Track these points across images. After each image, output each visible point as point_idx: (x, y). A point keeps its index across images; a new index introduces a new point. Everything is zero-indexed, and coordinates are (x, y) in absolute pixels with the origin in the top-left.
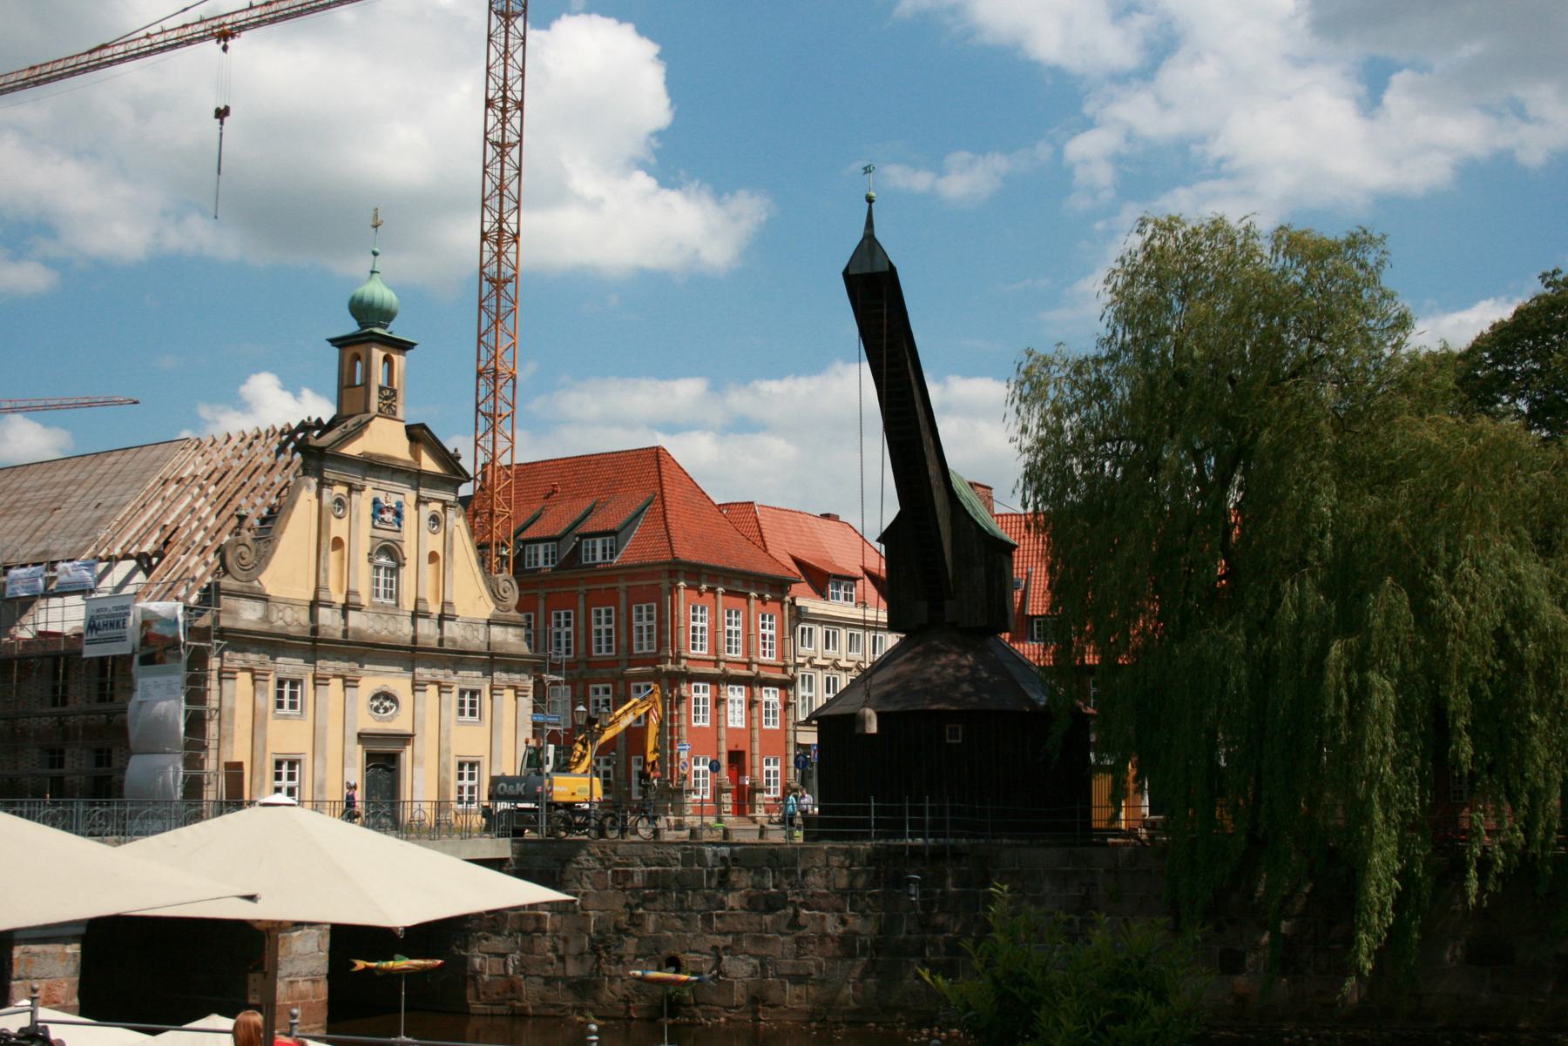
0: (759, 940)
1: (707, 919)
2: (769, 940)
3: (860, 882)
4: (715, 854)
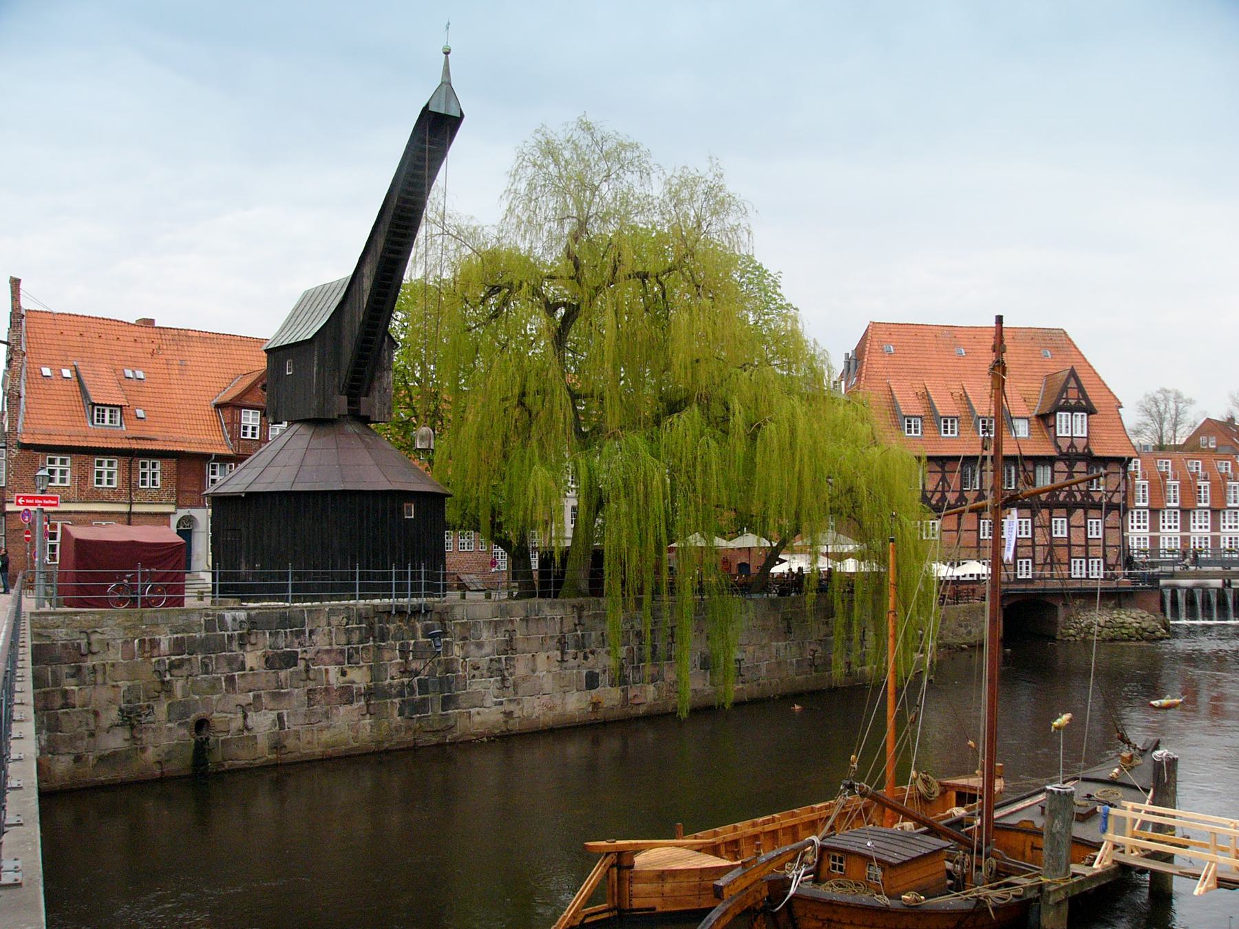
0: (276, 696)
1: (230, 680)
2: (285, 694)
3: (356, 637)
4: (234, 619)
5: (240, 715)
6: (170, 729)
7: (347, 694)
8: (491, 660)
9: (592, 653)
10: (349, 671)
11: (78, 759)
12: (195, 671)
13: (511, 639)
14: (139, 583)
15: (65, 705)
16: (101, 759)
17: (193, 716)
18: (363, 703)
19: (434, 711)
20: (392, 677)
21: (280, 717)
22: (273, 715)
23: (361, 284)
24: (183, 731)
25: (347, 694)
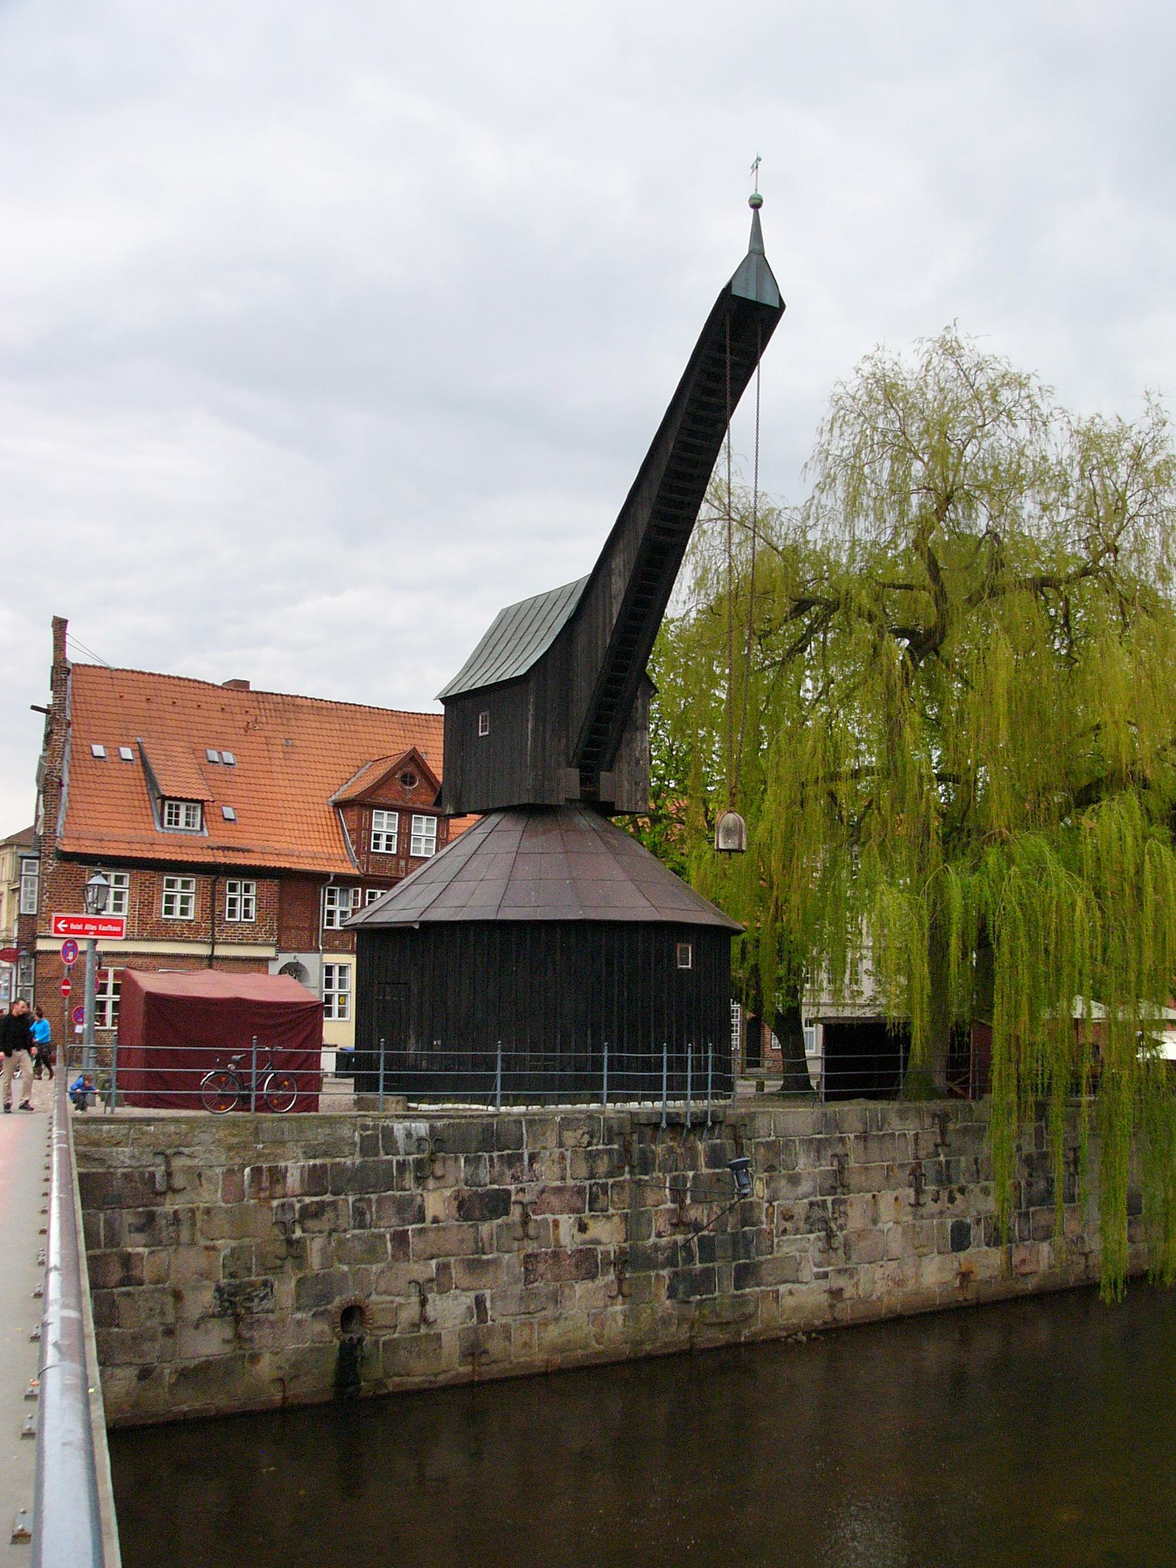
0: (475, 1266)
1: (400, 1239)
2: (489, 1262)
3: (603, 1166)
4: (409, 1135)
5: (415, 1299)
6: (299, 1323)
7: (587, 1263)
8: (811, 1204)
9: (962, 1190)
10: (591, 1223)
11: (145, 1374)
12: (343, 1223)
13: (841, 1170)
14: (254, 1071)
15: (127, 1281)
16: (185, 1375)
17: (337, 1300)
18: (611, 1277)
19: (725, 1290)
20: (659, 1234)
21: (480, 1302)
22: (468, 1299)
23: (608, 586)
24: (321, 1326)
25: (587, 1263)
